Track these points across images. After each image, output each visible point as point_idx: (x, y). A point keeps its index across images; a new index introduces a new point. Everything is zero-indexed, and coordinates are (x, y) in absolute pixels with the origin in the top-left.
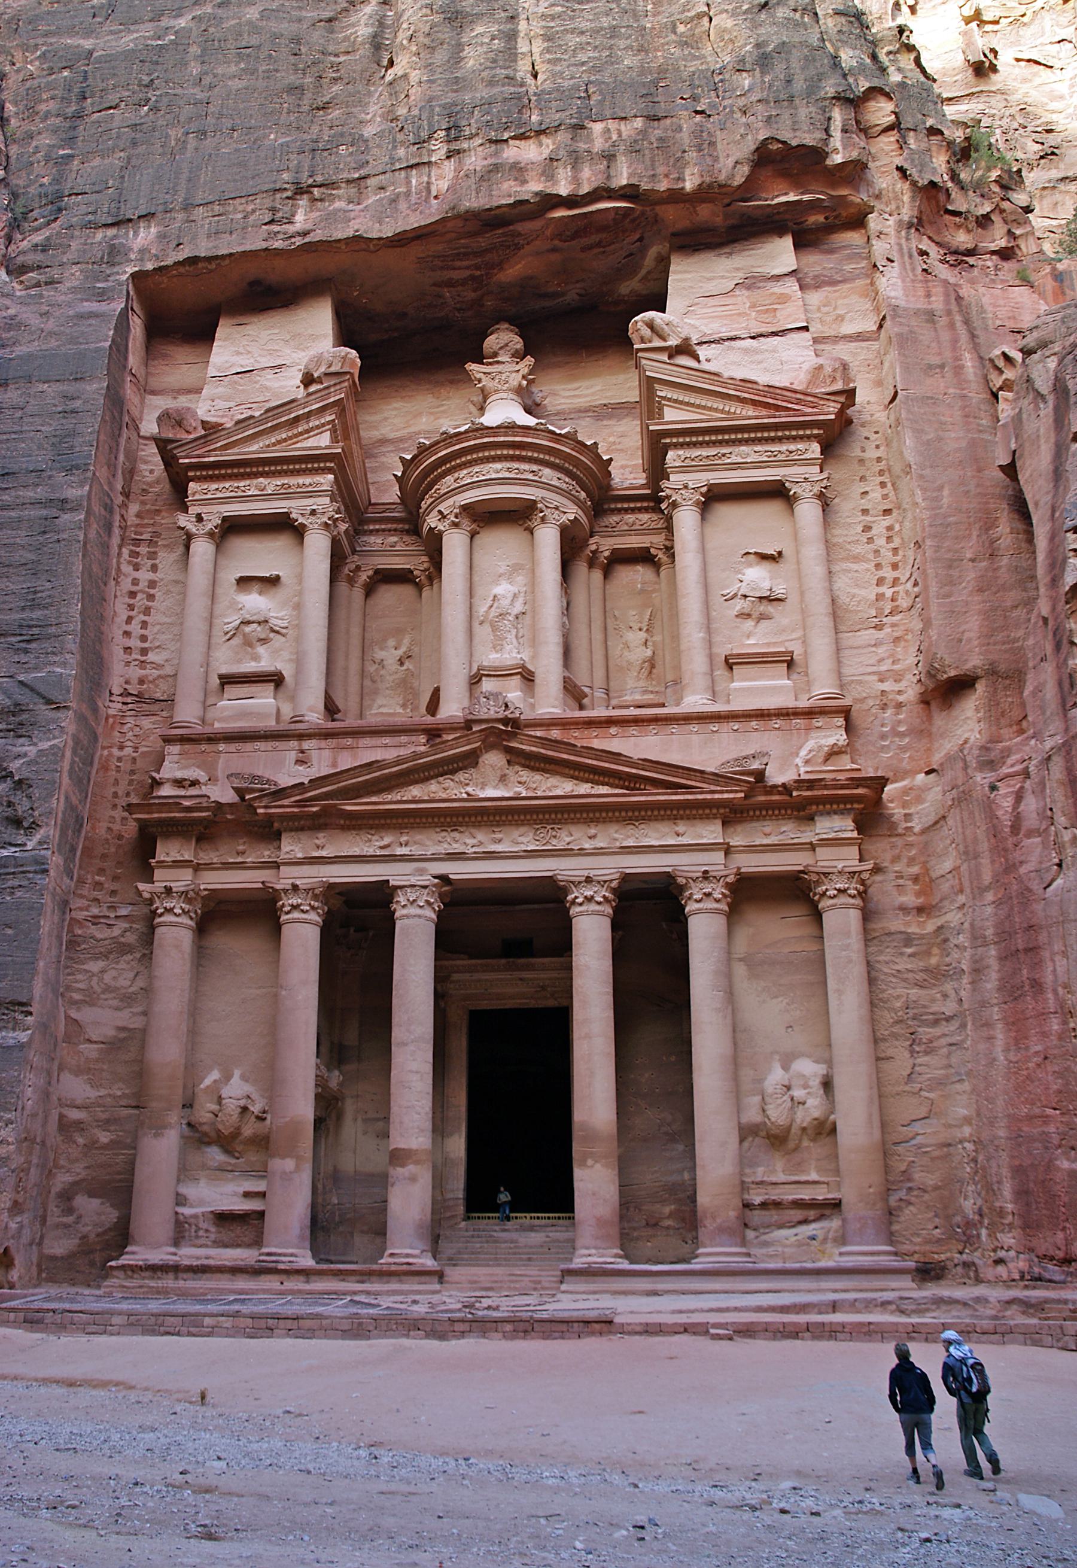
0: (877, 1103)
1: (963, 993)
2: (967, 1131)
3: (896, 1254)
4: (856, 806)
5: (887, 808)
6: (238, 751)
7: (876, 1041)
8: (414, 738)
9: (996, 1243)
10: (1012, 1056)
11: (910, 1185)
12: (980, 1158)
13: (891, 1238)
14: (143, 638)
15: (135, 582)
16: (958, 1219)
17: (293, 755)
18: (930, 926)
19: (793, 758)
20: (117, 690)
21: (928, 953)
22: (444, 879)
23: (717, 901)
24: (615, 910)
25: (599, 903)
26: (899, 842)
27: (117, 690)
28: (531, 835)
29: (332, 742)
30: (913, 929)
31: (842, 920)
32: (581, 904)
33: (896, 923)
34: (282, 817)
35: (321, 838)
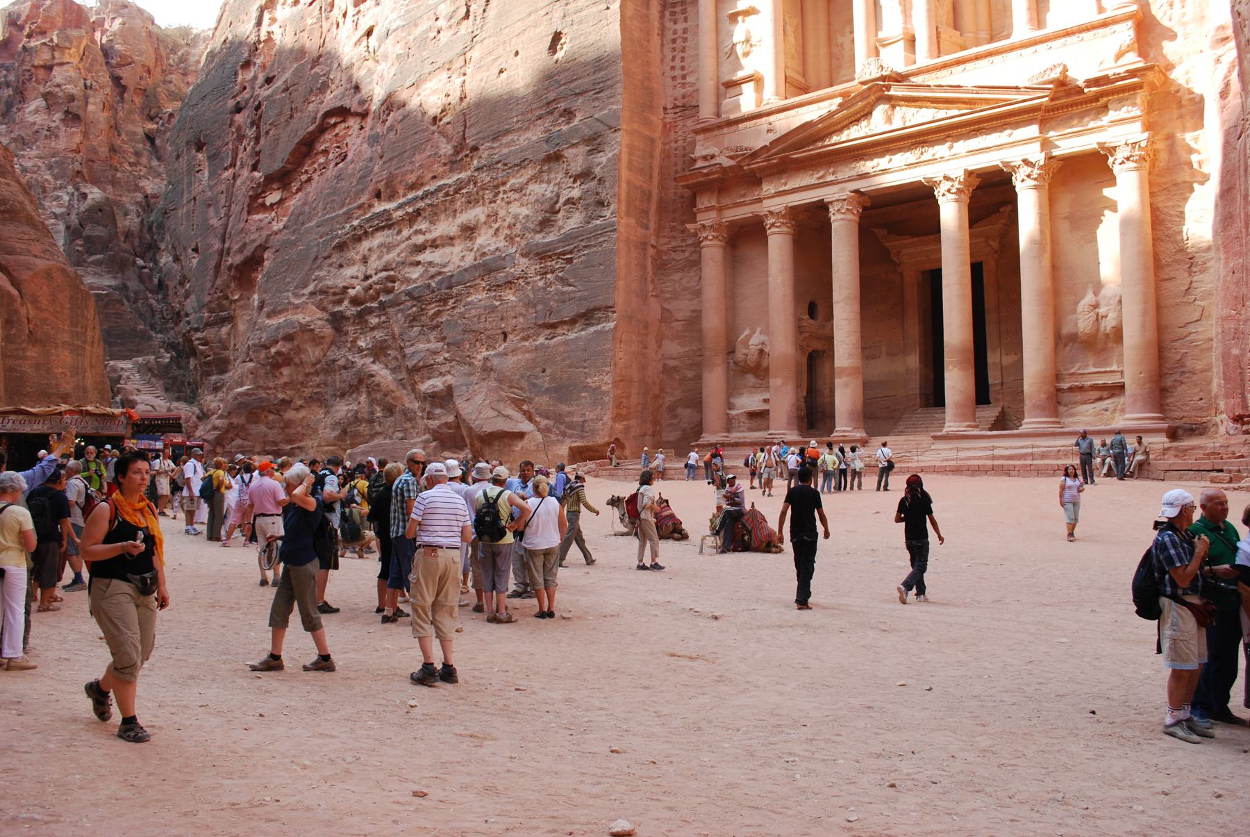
0: (1152, 312)
14: (683, 68)
15: (675, 32)
19: (1090, 60)
20: (669, 106)
22: (857, 191)
24: (973, 198)
26: (1183, 110)
27: (669, 106)
34: (759, 168)
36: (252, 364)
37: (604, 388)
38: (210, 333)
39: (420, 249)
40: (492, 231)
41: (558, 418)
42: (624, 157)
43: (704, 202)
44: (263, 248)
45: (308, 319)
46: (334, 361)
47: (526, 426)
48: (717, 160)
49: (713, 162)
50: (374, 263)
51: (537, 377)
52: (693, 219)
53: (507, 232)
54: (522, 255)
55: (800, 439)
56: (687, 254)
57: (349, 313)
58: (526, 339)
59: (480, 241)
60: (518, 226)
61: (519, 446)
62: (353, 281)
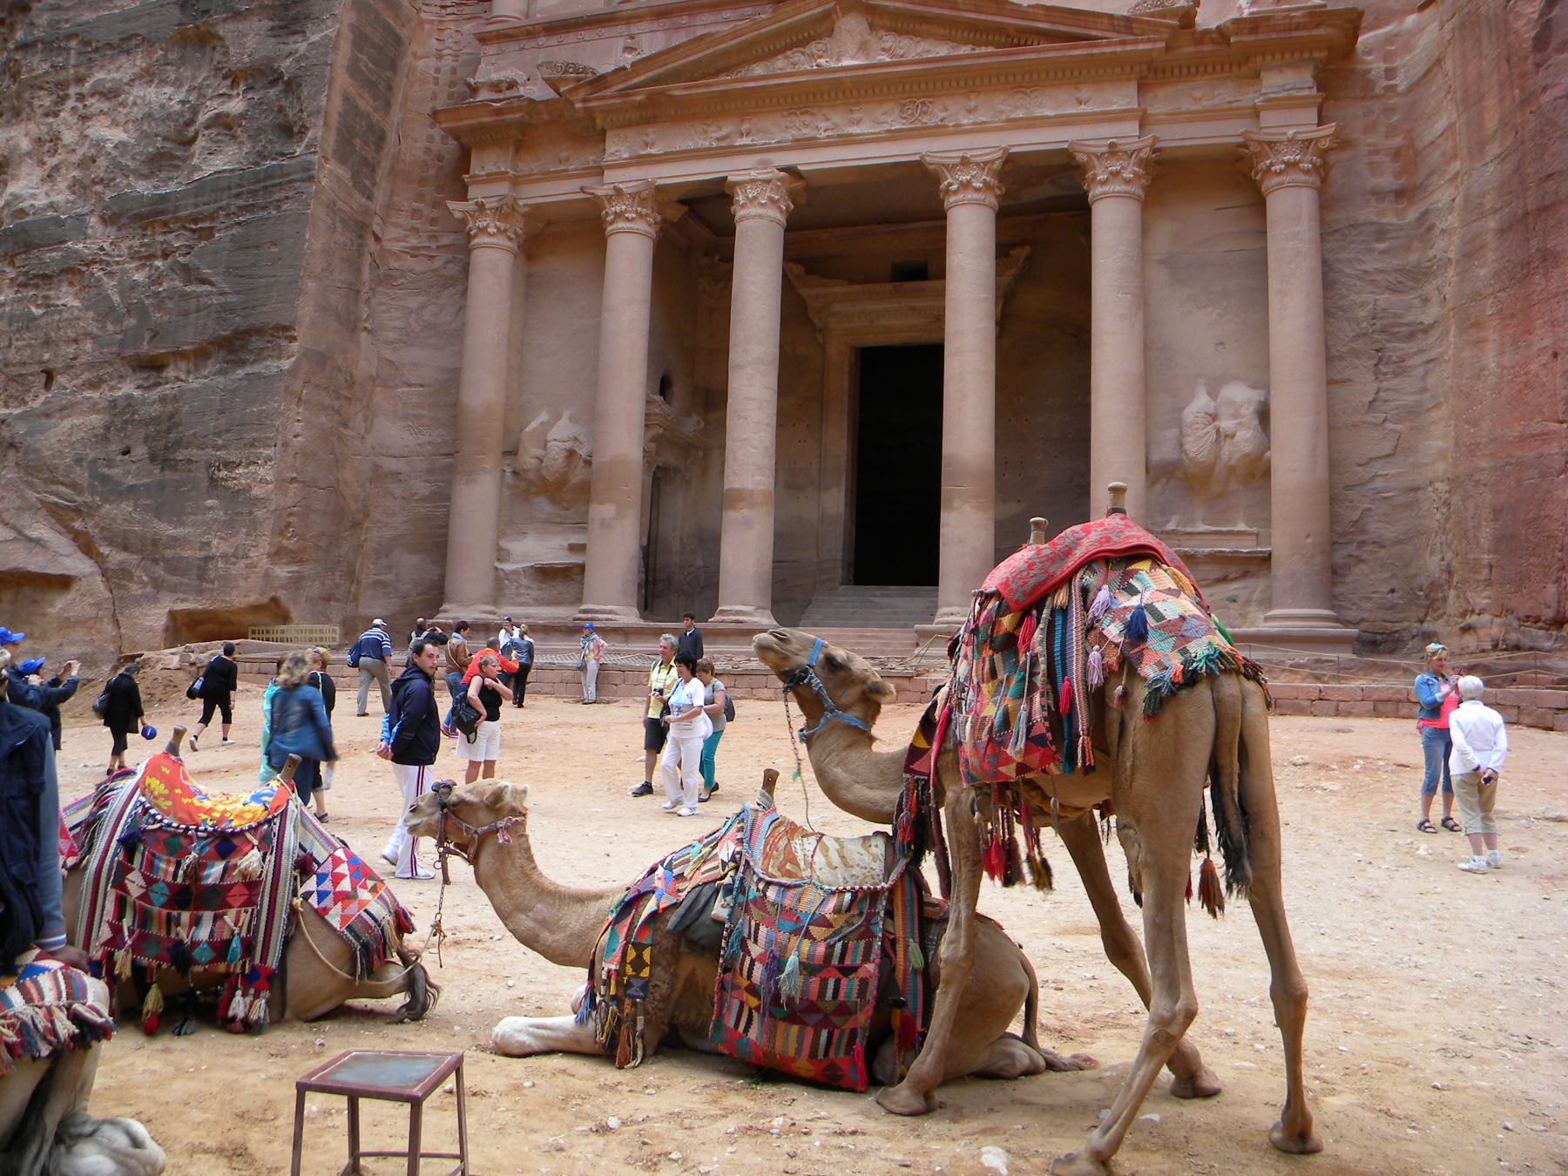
1: (1448, 290)
2: (1440, 468)
3: (1336, 620)
4: (1318, 55)
5: (1363, 62)
6: (560, 44)
7: (1330, 359)
8: (759, 9)
9: (1465, 606)
10: (1507, 360)
11: (1362, 538)
12: (1455, 499)
13: (1332, 601)
16: (1423, 580)
17: (621, 42)
18: (1412, 215)
21: (1407, 248)
22: (791, 171)
23: (1128, 182)
25: (977, 190)
26: (1376, 106)
28: (897, 112)
29: (665, 23)
30: (1390, 219)
31: (1291, 210)
32: (955, 192)
33: (1367, 213)
35: (651, 132)
37: (257, 491)
41: (151, 549)
42: (345, 47)
43: (483, 164)
47: (75, 564)
48: (522, 91)
49: (508, 94)
51: (110, 463)
52: (463, 197)
55: (642, 623)
56: (437, 263)
58: (93, 385)
60: (102, 162)
61: (59, 604)
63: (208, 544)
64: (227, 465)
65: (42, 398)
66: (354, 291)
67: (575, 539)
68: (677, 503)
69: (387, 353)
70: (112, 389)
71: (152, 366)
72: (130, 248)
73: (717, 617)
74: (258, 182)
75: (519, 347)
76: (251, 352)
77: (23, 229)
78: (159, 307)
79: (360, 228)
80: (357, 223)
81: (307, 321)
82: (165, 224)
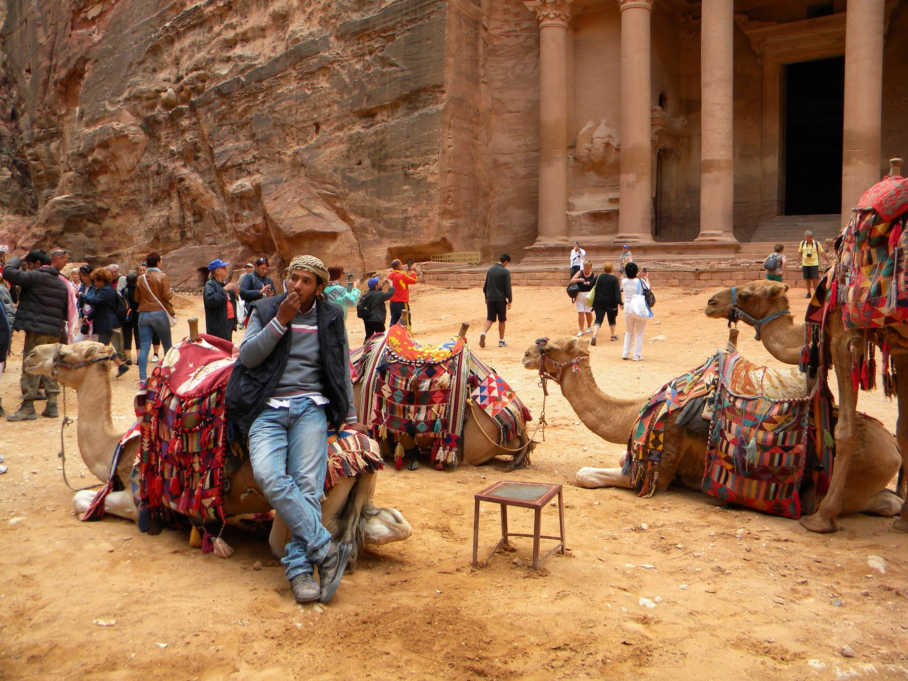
36: (71, 173)
37: (430, 179)
38: (41, 148)
39: (230, 44)
40: (303, 17)
44: (84, 60)
45: (121, 125)
46: (148, 167)
47: (338, 226)
50: (186, 63)
53: (321, 15)
54: (337, 38)
55: (654, 243)
57: (161, 117)
58: (340, 128)
59: (291, 28)
62: (166, 85)
63: (406, 210)
64: (414, 166)
65: (315, 138)
66: (475, 61)
67: (613, 195)
68: (673, 170)
69: (497, 95)
70: (349, 130)
71: (369, 115)
72: (352, 51)
73: (700, 238)
74: (416, 4)
75: (573, 84)
76: (421, 102)
77: (298, 49)
78: (370, 82)
79: (476, 24)
80: (473, 21)
81: (450, 81)
82: (369, 35)
